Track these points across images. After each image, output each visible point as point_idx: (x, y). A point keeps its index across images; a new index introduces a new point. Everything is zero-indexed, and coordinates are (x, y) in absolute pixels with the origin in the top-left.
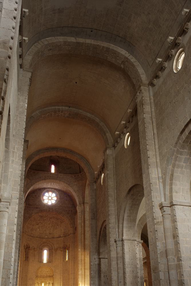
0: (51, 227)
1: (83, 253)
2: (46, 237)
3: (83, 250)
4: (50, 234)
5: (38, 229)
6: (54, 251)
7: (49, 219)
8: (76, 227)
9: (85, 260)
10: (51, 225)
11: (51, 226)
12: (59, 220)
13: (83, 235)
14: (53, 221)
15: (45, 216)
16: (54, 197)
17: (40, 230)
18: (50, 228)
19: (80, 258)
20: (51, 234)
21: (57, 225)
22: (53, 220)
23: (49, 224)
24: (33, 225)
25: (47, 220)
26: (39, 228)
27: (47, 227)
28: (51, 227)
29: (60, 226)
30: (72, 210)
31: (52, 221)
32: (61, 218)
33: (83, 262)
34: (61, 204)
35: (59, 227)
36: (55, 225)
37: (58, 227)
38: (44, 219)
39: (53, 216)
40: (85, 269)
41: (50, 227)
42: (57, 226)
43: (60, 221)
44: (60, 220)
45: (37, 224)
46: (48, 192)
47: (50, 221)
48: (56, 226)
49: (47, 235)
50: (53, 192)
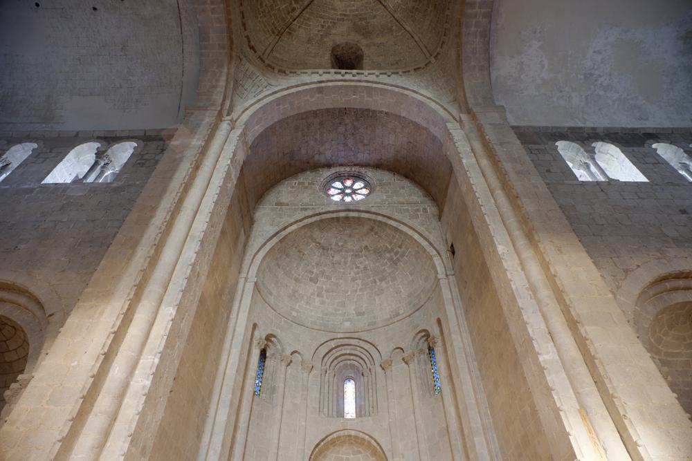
0: (361, 290)
1: (528, 254)
2: (347, 324)
3: (522, 242)
4: (359, 314)
5: (317, 299)
6: (379, 370)
7: (349, 259)
8: (452, 245)
9: (551, 279)
10: (359, 282)
11: (360, 286)
12: (388, 255)
13: (499, 193)
14: (365, 268)
15: (337, 244)
16: (361, 189)
17: (323, 303)
18: (358, 293)
19: (517, 281)
20: (363, 314)
21: (381, 280)
22: (367, 263)
23: (353, 280)
24: (297, 280)
25: (345, 263)
26: (318, 296)
27: (349, 293)
28: (361, 290)
29: (394, 279)
30: (425, 209)
31: (362, 267)
32: (391, 243)
33: (545, 293)
34: (385, 197)
35: (390, 283)
36: (375, 282)
37: (384, 285)
38: (335, 259)
39: (365, 243)
40: (573, 325)
41: (356, 291)
42: (383, 283)
43: (391, 259)
44: (389, 252)
45: (311, 280)
46: (340, 177)
47: (358, 267)
48: (378, 283)
49: (349, 320)
50: (357, 177)
